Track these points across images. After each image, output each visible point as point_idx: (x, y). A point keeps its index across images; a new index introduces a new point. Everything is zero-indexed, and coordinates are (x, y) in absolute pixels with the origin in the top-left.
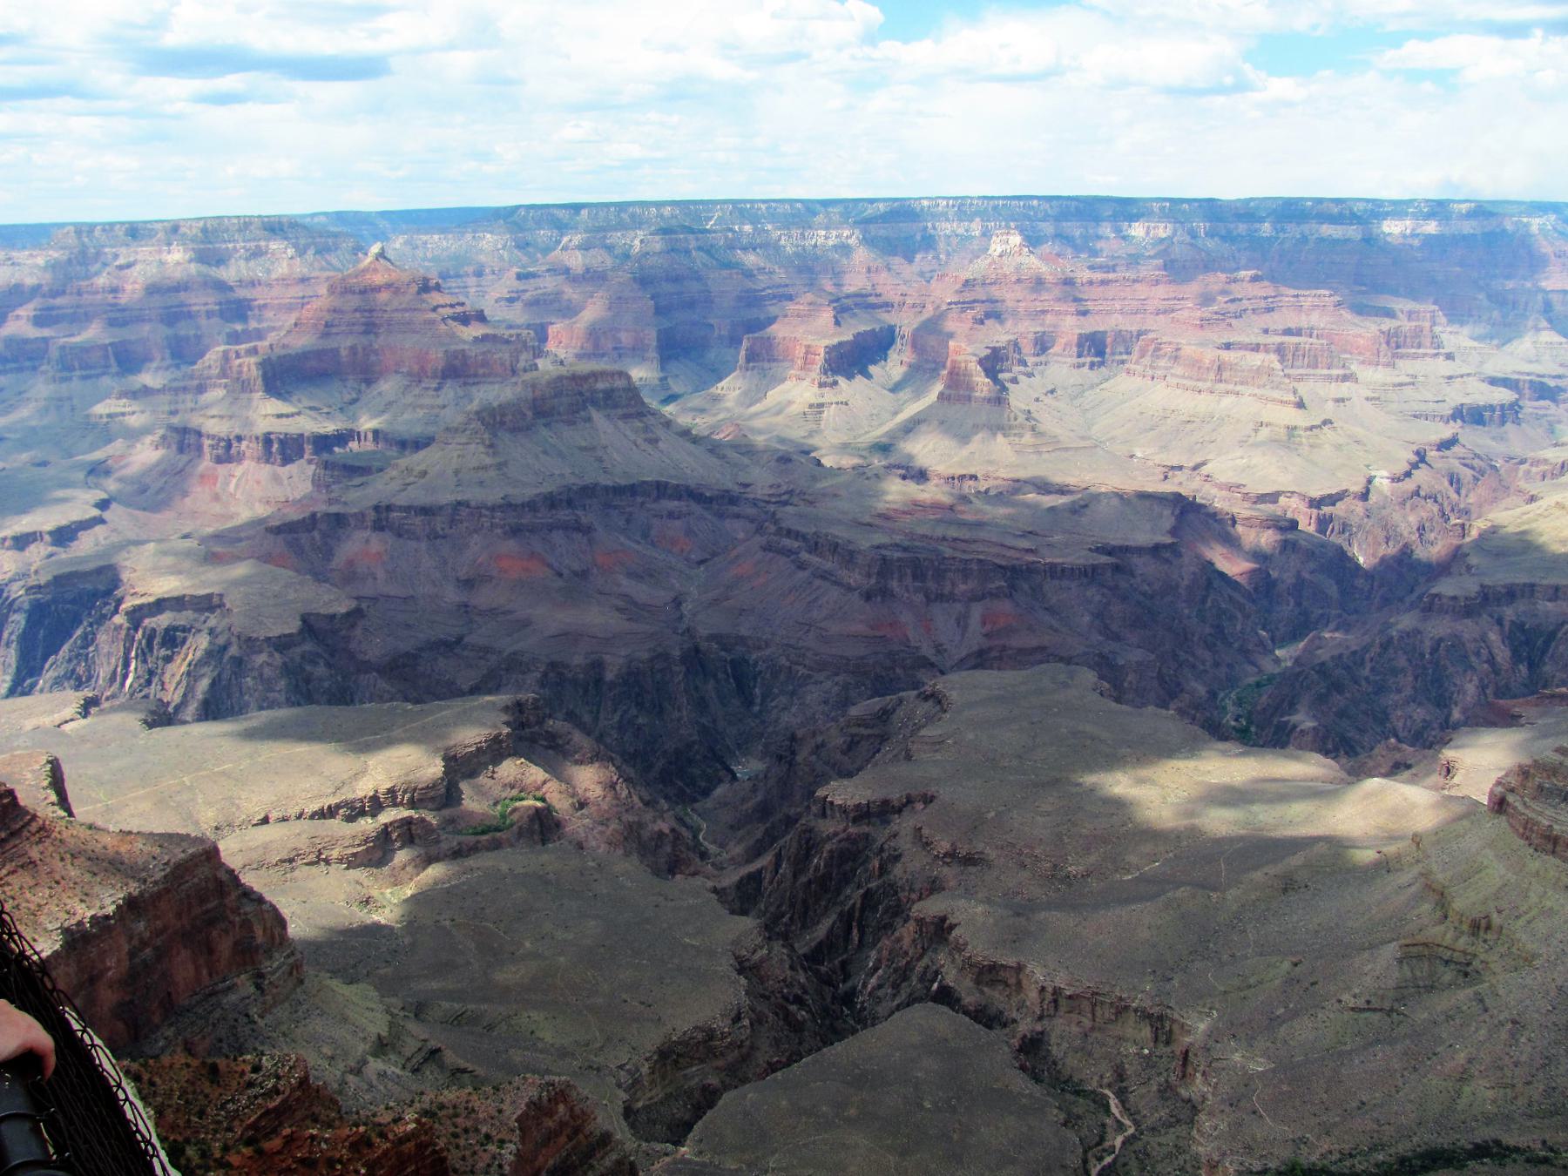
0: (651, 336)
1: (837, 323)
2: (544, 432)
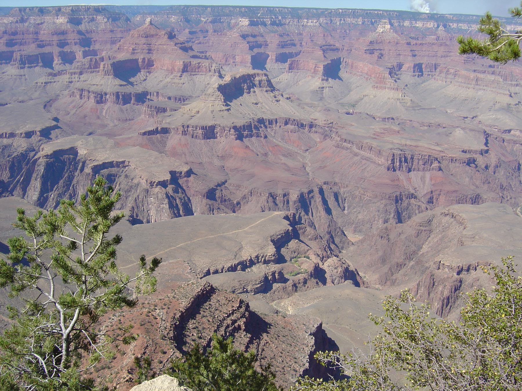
0: (249, 58)
1: (325, 56)
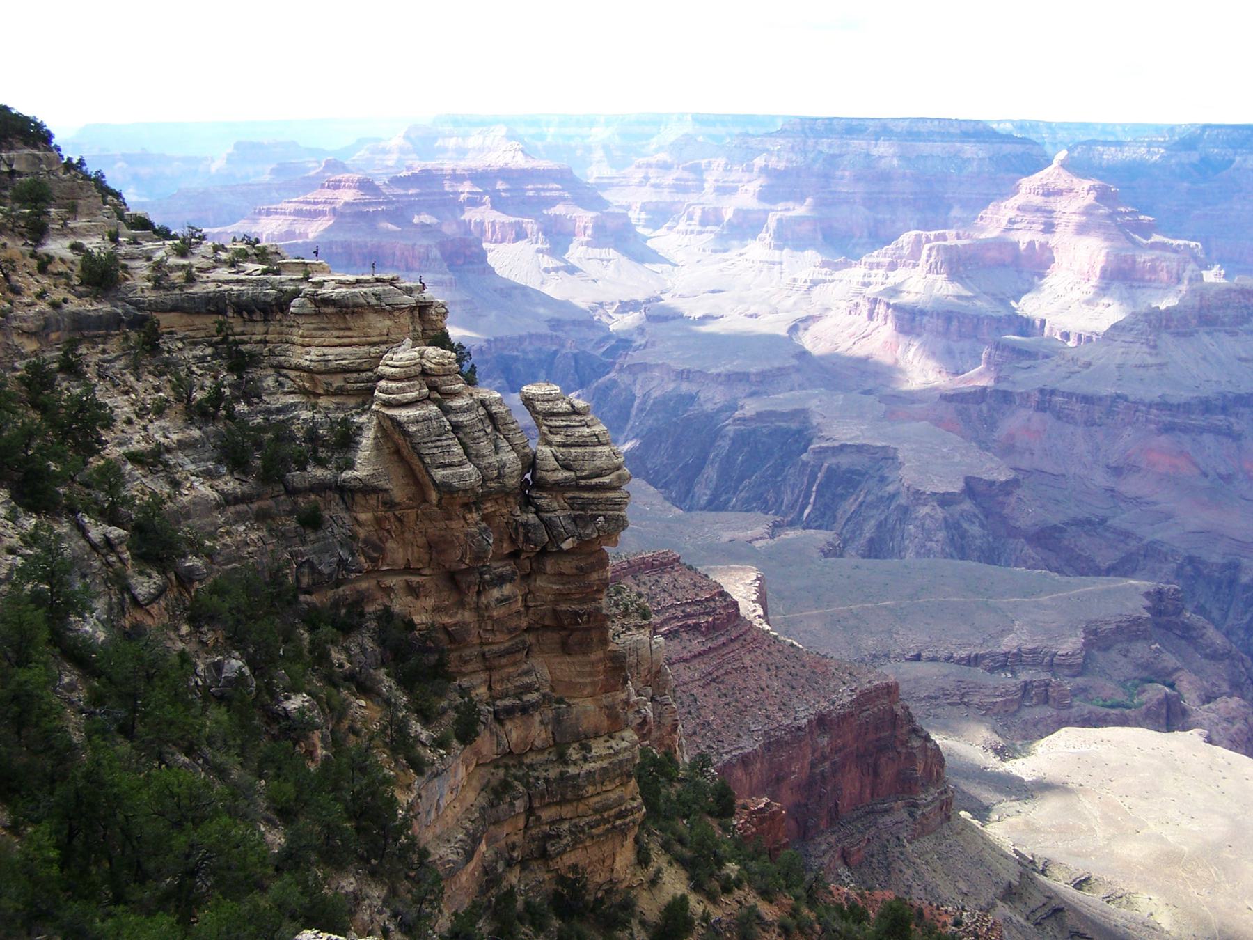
2: (1206, 339)
